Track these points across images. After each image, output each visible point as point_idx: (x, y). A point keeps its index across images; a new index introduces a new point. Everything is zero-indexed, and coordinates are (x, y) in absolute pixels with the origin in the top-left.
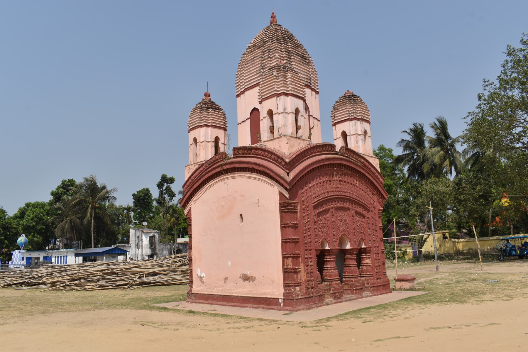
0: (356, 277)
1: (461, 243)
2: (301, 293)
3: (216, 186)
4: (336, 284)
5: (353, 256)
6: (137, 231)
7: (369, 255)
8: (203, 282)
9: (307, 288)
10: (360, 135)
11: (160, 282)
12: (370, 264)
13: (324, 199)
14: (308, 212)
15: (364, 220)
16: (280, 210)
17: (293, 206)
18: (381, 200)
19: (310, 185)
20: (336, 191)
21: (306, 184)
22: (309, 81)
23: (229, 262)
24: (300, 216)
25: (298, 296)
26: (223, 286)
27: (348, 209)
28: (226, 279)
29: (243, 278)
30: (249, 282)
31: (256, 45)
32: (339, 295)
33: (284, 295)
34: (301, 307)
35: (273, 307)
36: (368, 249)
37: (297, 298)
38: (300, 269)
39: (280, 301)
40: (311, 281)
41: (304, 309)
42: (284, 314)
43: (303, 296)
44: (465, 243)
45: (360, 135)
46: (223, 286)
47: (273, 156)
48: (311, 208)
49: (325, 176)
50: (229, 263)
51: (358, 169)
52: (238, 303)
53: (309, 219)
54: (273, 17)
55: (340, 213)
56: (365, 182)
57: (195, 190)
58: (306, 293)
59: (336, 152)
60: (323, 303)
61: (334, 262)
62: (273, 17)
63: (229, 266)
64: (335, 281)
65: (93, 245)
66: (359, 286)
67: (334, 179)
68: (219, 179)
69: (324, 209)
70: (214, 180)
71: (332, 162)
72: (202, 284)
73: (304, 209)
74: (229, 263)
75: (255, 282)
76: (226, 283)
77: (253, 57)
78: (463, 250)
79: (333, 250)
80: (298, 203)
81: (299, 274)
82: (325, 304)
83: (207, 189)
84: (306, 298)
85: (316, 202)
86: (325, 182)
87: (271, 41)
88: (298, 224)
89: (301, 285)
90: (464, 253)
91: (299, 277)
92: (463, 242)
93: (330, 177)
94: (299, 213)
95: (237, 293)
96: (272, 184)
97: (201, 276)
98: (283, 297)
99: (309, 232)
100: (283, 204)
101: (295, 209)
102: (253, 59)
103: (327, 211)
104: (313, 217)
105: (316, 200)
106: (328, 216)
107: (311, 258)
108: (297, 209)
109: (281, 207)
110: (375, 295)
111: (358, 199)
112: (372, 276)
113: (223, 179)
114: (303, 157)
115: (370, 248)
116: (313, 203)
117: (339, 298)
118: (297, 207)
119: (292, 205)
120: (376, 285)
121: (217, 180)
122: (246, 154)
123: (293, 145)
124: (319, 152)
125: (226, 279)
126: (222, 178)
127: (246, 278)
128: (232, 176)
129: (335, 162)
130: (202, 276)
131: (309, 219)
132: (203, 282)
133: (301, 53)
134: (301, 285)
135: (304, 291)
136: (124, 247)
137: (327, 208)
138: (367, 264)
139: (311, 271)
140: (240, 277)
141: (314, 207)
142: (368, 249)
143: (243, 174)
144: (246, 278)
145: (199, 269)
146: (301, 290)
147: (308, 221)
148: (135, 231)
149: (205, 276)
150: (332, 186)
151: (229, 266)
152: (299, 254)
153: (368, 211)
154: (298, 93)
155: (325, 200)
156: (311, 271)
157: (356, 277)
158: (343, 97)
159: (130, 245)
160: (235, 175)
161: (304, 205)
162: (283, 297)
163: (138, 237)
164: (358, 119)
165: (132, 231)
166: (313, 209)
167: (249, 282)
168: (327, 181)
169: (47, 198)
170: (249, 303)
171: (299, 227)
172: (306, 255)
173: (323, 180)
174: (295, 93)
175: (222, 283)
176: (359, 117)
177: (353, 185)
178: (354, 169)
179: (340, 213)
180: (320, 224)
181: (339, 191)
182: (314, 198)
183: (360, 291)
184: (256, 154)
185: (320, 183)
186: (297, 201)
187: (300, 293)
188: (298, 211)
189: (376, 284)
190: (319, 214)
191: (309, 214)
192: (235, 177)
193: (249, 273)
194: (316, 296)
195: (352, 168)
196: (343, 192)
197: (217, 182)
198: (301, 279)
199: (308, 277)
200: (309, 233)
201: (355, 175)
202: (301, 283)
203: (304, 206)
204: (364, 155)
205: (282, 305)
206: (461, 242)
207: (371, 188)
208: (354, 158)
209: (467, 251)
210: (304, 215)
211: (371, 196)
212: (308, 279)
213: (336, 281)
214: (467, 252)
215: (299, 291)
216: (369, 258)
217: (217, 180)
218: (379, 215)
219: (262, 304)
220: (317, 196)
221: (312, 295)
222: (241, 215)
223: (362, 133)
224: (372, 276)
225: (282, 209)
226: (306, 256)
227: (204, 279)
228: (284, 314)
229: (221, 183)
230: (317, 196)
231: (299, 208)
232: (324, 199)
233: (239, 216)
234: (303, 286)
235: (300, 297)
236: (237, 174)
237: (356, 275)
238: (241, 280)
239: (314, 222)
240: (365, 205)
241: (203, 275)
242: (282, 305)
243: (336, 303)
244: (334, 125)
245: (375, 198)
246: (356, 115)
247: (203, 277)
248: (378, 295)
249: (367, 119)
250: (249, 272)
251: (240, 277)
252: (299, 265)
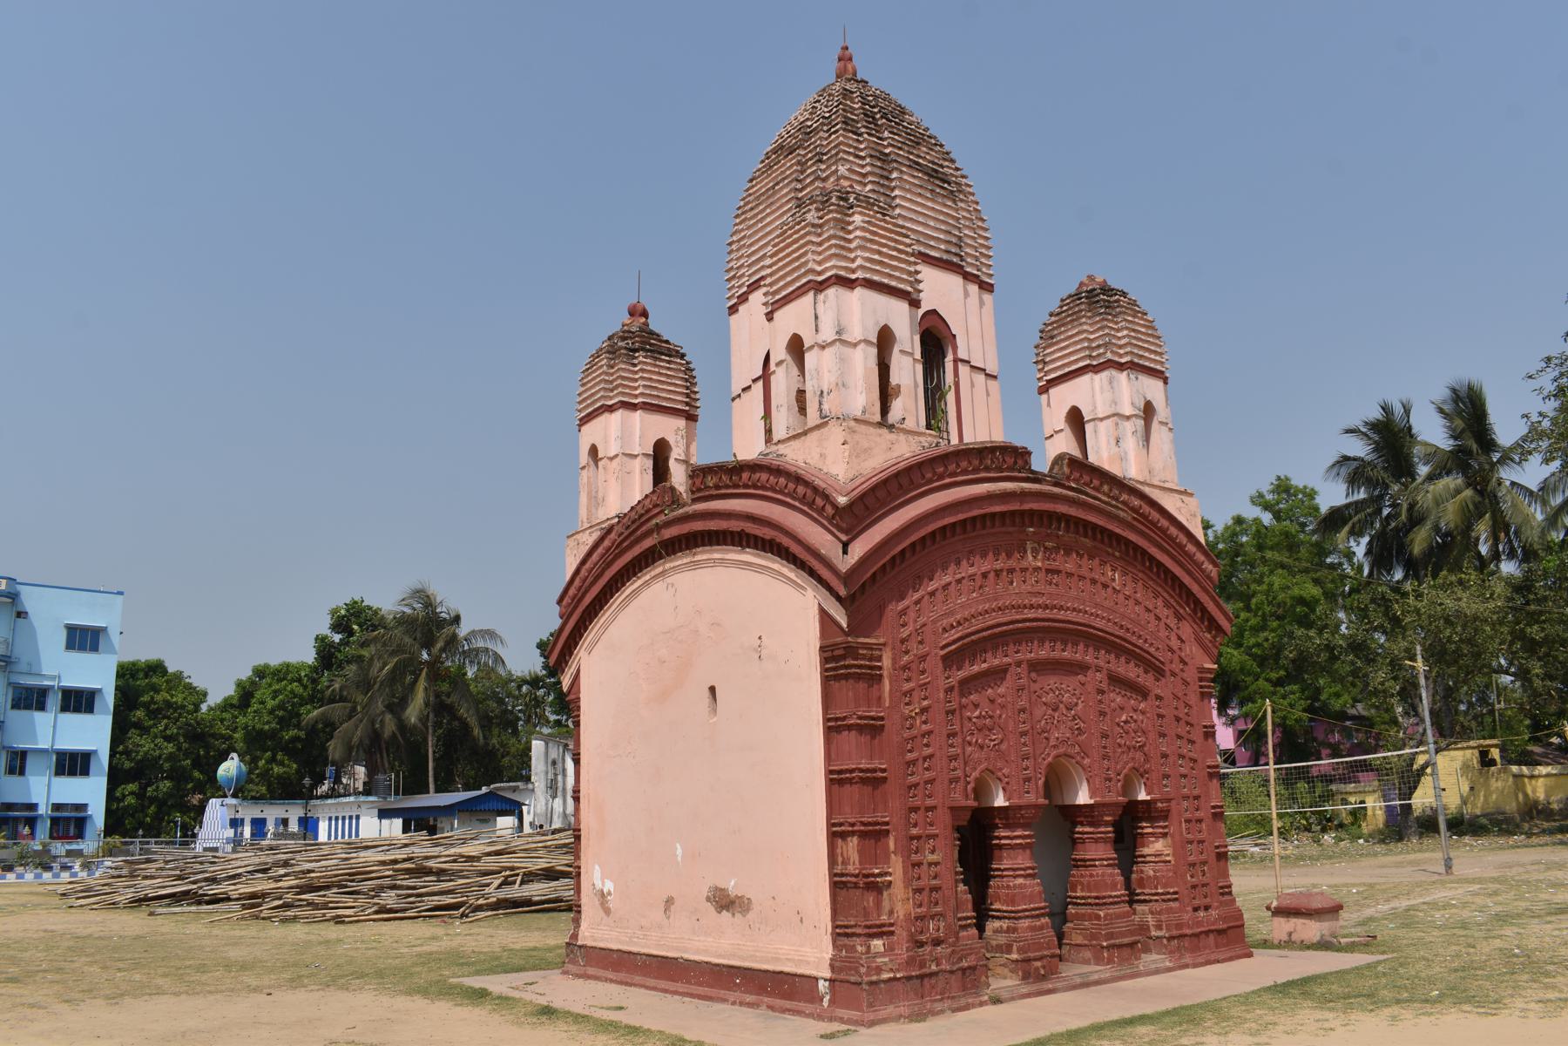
0: (1111, 903)
1: (1541, 780)
2: (891, 961)
3: (646, 595)
4: (1033, 929)
5: (1102, 829)
6: (550, 745)
7: (1166, 827)
8: (607, 911)
9: (917, 942)
10: (1128, 418)
11: (562, 901)
12: (1168, 858)
13: (984, 634)
14: (924, 679)
15: (1142, 705)
16: (824, 670)
17: (864, 657)
18: (1209, 636)
19: (932, 586)
20: (1032, 607)
21: (917, 581)
22: (953, 250)
23: (678, 846)
24: (891, 690)
25: (879, 970)
27: (1082, 668)
28: (669, 902)
29: (717, 902)
30: (734, 915)
32: (1044, 967)
33: (832, 967)
34: (890, 1010)
35: (801, 1005)
36: (1159, 805)
37: (874, 978)
38: (890, 874)
39: (823, 986)
40: (932, 917)
41: (901, 1016)
42: (822, 1036)
43: (898, 970)
44: (1553, 779)
45: (1128, 418)
47: (801, 490)
48: (934, 664)
49: (991, 554)
50: (679, 851)
51: (1118, 531)
52: (700, 984)
53: (925, 703)
54: (845, 58)
55: (1052, 682)
56: (1146, 574)
57: (590, 613)
58: (910, 962)
59: (1033, 472)
60: (978, 995)
61: (1028, 852)
62: (845, 58)
63: (679, 859)
64: (1027, 917)
65: (432, 787)
66: (1122, 935)
67: (1024, 564)
68: (653, 573)
69: (984, 666)
70: (639, 578)
71: (1014, 506)
72: (605, 917)
73: (905, 668)
74: (679, 851)
75: (751, 915)
76: (668, 918)
77: (771, 184)
78: (1549, 803)
79: (1020, 807)
80: (884, 645)
81: (885, 893)
82: (986, 998)
84: (909, 978)
85: (954, 642)
86: (992, 575)
87: (825, 128)
88: (882, 719)
89: (892, 933)
90: (1552, 810)
91: (886, 904)
92: (1548, 775)
93: (1009, 556)
94: (886, 682)
95: (698, 952)
96: (799, 581)
97: (602, 891)
98: (828, 975)
99: (927, 745)
100: (832, 651)
101: (871, 668)
102: (773, 187)
103: (999, 674)
104: (942, 695)
105: (956, 636)
106: (1001, 690)
107: (934, 836)
108: (880, 668)
109: (825, 660)
110: (1186, 966)
111: (1121, 633)
112: (1176, 899)
114: (903, 490)
115: (1169, 800)
116: (943, 648)
117: (1044, 978)
118: (879, 659)
119: (861, 652)
120: (1188, 932)
121: (647, 576)
122: (727, 487)
123: (866, 450)
124: (965, 472)
125: (669, 902)
126: (660, 569)
127: (725, 902)
128: (688, 560)
129: (1027, 506)
130: (605, 891)
131: (925, 703)
132: (607, 911)
133: (930, 162)
134: (892, 933)
135: (903, 952)
136: (514, 791)
137: (996, 662)
138: (1156, 856)
139: (934, 882)
140: (708, 899)
141: (945, 658)
142: (1159, 805)
143: (717, 553)
144: (725, 902)
145: (597, 867)
146: (892, 949)
147: (924, 710)
148: (547, 744)
149: (612, 890)
150: (1018, 590)
151: (679, 859)
152: (887, 823)
153: (1159, 672)
154: (890, 276)
155: (990, 636)
156: (934, 882)
157: (1111, 903)
158: (1070, 296)
159: (530, 786)
160: (696, 559)
161: (907, 652)
162: (828, 975)
163: (554, 763)
164: (1121, 367)
165: (537, 746)
166: (941, 665)
167: (734, 915)
168: (998, 573)
169: (307, 655)
170: (731, 987)
171: (886, 729)
172: (915, 825)
173: (983, 569)
174: (876, 278)
175: (658, 915)
176: (1123, 360)
177: (1099, 584)
178: (1103, 530)
179: (1052, 682)
180: (970, 719)
181: (1046, 607)
182: (945, 630)
183: (1126, 952)
184: (755, 487)
185: (972, 577)
186: (882, 641)
187: (887, 959)
188: (885, 673)
189: (1189, 927)
190: (966, 685)
191: (929, 683)
192: (695, 565)
193: (732, 886)
194: (952, 972)
195: (1095, 527)
196: (1061, 608)
197: (647, 584)
198: (891, 912)
199: (920, 906)
200: (927, 751)
201: (1109, 554)
202: (892, 925)
203: (906, 658)
204: (1141, 483)
205: (826, 1003)
206: (1539, 776)
207: (1170, 595)
208: (1104, 494)
209: (1561, 806)
210: (907, 686)
211: (1172, 622)
212: (919, 910)
213: (1032, 917)
214: (1561, 810)
215: (882, 955)
216: (1165, 835)
217: (648, 577)
218: (1201, 687)
219: (769, 995)
220: (959, 623)
221: (934, 967)
222: (712, 689)
223: (1137, 412)
224: (1176, 899)
225: (828, 666)
226: (914, 831)
227: (612, 902)
228: (822, 1036)
229: (658, 587)
230: (959, 623)
231: (886, 662)
232: (984, 634)
233: (707, 693)
234: (901, 934)
235: (885, 976)
236: (703, 555)
237: (1110, 897)
238: (710, 908)
239: (947, 713)
240: (1148, 653)
241: (609, 886)
242: (826, 1003)
243: (1028, 995)
244: (1043, 390)
245: (1187, 629)
246: (1112, 352)
247: (609, 893)
248: (1195, 966)
249: (1152, 365)
250: (732, 883)
251: (708, 899)
252: (887, 861)
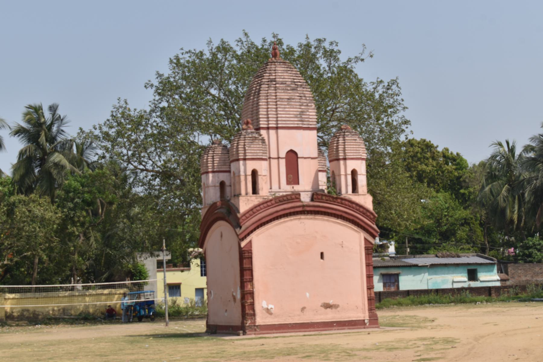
8: (271, 314)
16: (365, 252)
26: (299, 315)
31: (286, 84)
33: (369, 317)
35: (359, 327)
39: (366, 321)
46: (299, 315)
47: (361, 210)
50: (308, 294)
52: (320, 328)
74: (308, 294)
75: (339, 309)
83: (277, 225)
95: (318, 319)
98: (368, 319)
109: (365, 250)
113: (300, 219)
121: (292, 218)
122: (331, 201)
127: (327, 306)
132: (271, 314)
143: (326, 218)
144: (327, 306)
162: (368, 319)
170: (333, 326)
184: (342, 204)
197: (291, 220)
205: (368, 324)
219: (347, 326)
222: (322, 254)
227: (272, 311)
229: (296, 222)
238: (323, 309)
241: (270, 306)
242: (368, 324)
247: (272, 308)
251: (321, 306)
